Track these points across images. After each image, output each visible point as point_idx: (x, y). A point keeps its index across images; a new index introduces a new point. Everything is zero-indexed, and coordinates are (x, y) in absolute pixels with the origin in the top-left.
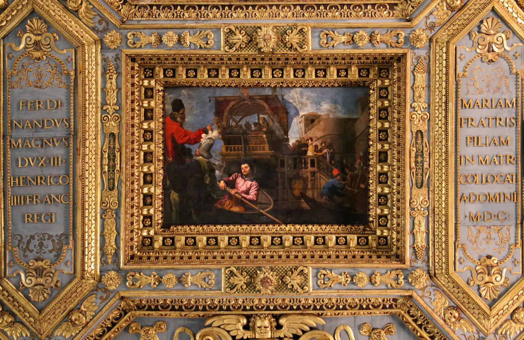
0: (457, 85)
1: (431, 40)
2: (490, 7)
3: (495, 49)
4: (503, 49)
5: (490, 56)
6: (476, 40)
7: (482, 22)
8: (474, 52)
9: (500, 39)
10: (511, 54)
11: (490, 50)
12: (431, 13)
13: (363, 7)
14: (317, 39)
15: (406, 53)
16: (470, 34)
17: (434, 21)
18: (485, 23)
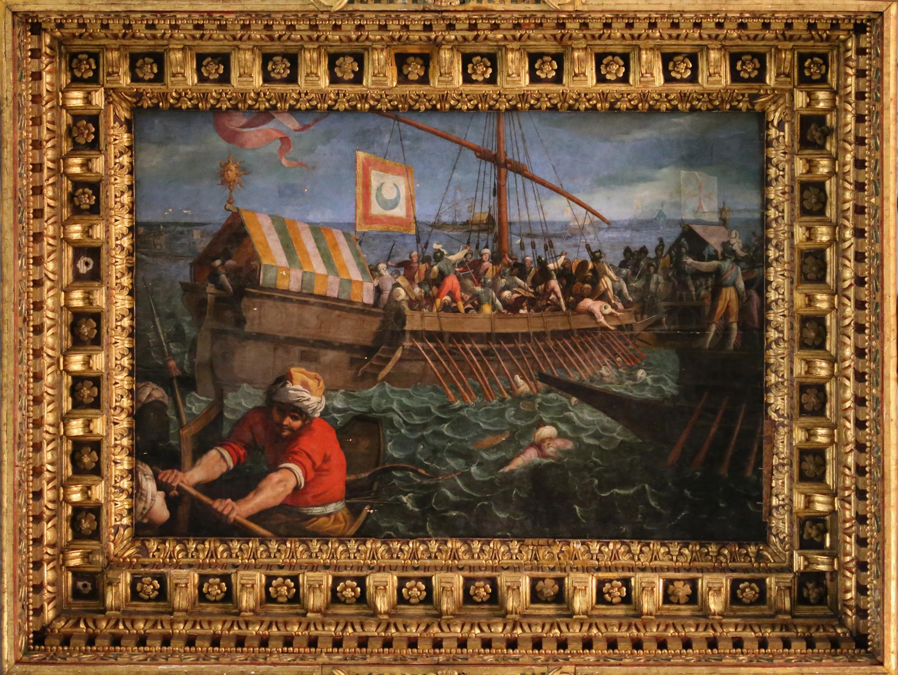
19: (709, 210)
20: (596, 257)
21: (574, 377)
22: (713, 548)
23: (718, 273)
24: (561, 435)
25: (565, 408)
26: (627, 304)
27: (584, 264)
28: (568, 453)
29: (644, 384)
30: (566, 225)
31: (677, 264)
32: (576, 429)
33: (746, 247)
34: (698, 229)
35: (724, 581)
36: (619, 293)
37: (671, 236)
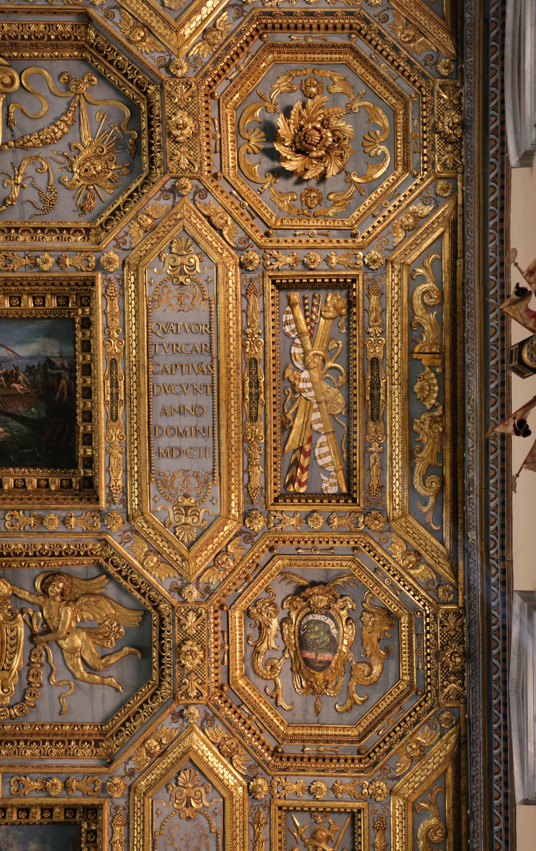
0: (153, 843)
1: (130, 788)
2: (186, 757)
3: (194, 804)
4: (201, 805)
5: (188, 812)
6: (173, 794)
7: (179, 774)
8: (171, 808)
9: (198, 793)
10: (211, 809)
11: (188, 805)
12: (130, 759)
13: (67, 743)
14: (8, 786)
15: (102, 804)
16: (166, 786)
17: (133, 766)
18: (182, 775)
19: (56, 352)
20: (17, 369)
21: (10, 411)
22: (58, 470)
23: (60, 374)
24: (6, 431)
25: (7, 422)
26: (27, 385)
27: (12, 371)
28: (8, 437)
29: (34, 413)
30: (5, 358)
31: (45, 371)
32: (10, 428)
33: (69, 365)
34: (52, 359)
35: (58, 481)
36: (25, 381)
37: (43, 361)
